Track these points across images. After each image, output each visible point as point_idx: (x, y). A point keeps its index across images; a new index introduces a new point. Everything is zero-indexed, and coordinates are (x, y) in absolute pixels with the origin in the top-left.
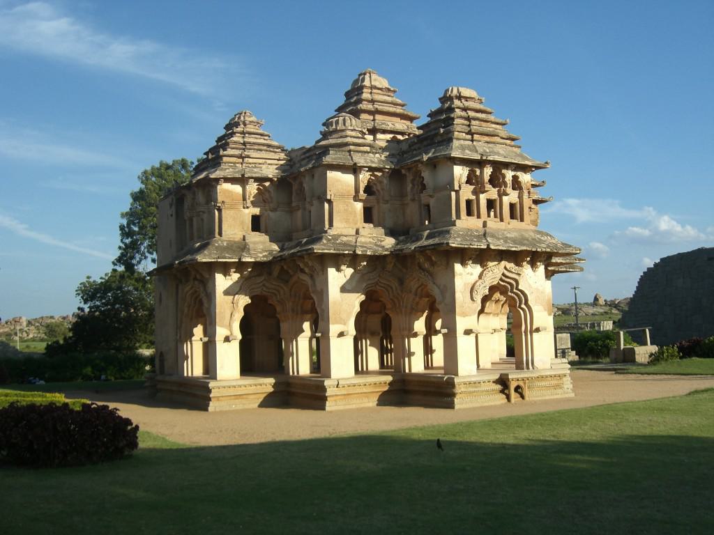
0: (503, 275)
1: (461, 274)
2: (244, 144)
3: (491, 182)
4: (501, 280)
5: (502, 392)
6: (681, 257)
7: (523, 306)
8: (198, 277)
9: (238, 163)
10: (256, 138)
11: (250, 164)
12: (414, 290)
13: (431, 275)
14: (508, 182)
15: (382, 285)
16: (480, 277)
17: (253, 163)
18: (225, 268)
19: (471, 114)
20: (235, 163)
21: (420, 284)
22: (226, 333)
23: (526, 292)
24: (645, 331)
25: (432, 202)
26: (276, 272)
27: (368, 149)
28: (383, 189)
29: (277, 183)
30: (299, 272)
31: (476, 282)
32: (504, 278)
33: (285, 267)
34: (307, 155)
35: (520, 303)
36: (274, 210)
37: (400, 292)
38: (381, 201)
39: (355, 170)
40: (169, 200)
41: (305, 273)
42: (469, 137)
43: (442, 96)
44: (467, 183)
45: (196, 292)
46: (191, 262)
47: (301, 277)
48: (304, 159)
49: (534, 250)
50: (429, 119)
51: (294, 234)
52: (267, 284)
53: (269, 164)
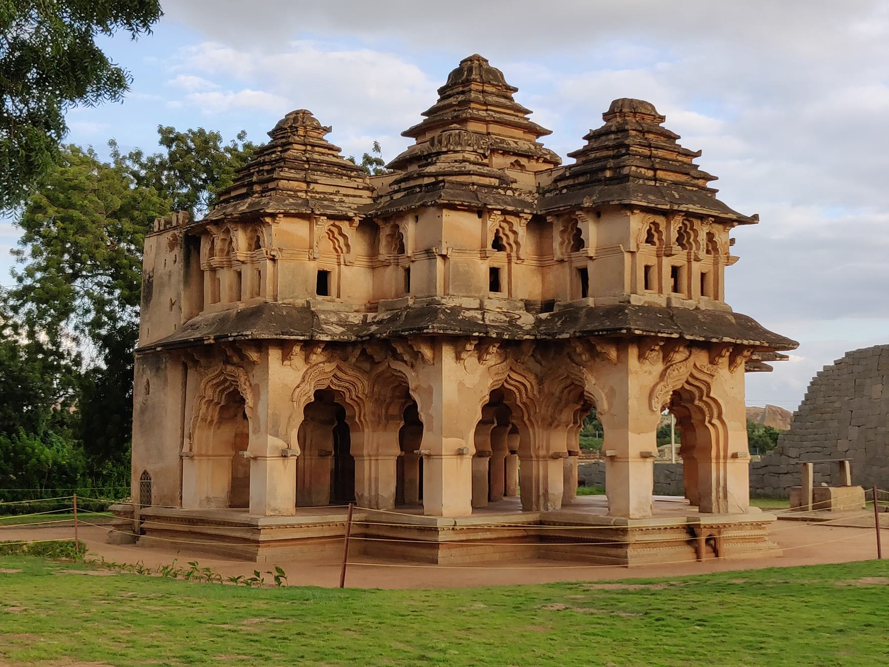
0: (692, 375)
1: (636, 373)
3: (679, 240)
4: (687, 382)
5: (689, 543)
7: (715, 421)
9: (301, 191)
10: (323, 154)
11: (318, 193)
12: (557, 394)
14: (701, 243)
15: (512, 382)
17: (322, 193)
21: (569, 382)
22: (281, 443)
23: (720, 401)
24: (842, 464)
25: (591, 268)
27: (496, 182)
30: (389, 358)
31: (657, 384)
32: (691, 380)
35: (711, 417)
38: (514, 259)
40: (168, 236)
42: (650, 173)
43: (607, 110)
44: (647, 242)
45: (225, 380)
49: (739, 342)
50: (586, 143)
52: (339, 374)
53: (344, 195)
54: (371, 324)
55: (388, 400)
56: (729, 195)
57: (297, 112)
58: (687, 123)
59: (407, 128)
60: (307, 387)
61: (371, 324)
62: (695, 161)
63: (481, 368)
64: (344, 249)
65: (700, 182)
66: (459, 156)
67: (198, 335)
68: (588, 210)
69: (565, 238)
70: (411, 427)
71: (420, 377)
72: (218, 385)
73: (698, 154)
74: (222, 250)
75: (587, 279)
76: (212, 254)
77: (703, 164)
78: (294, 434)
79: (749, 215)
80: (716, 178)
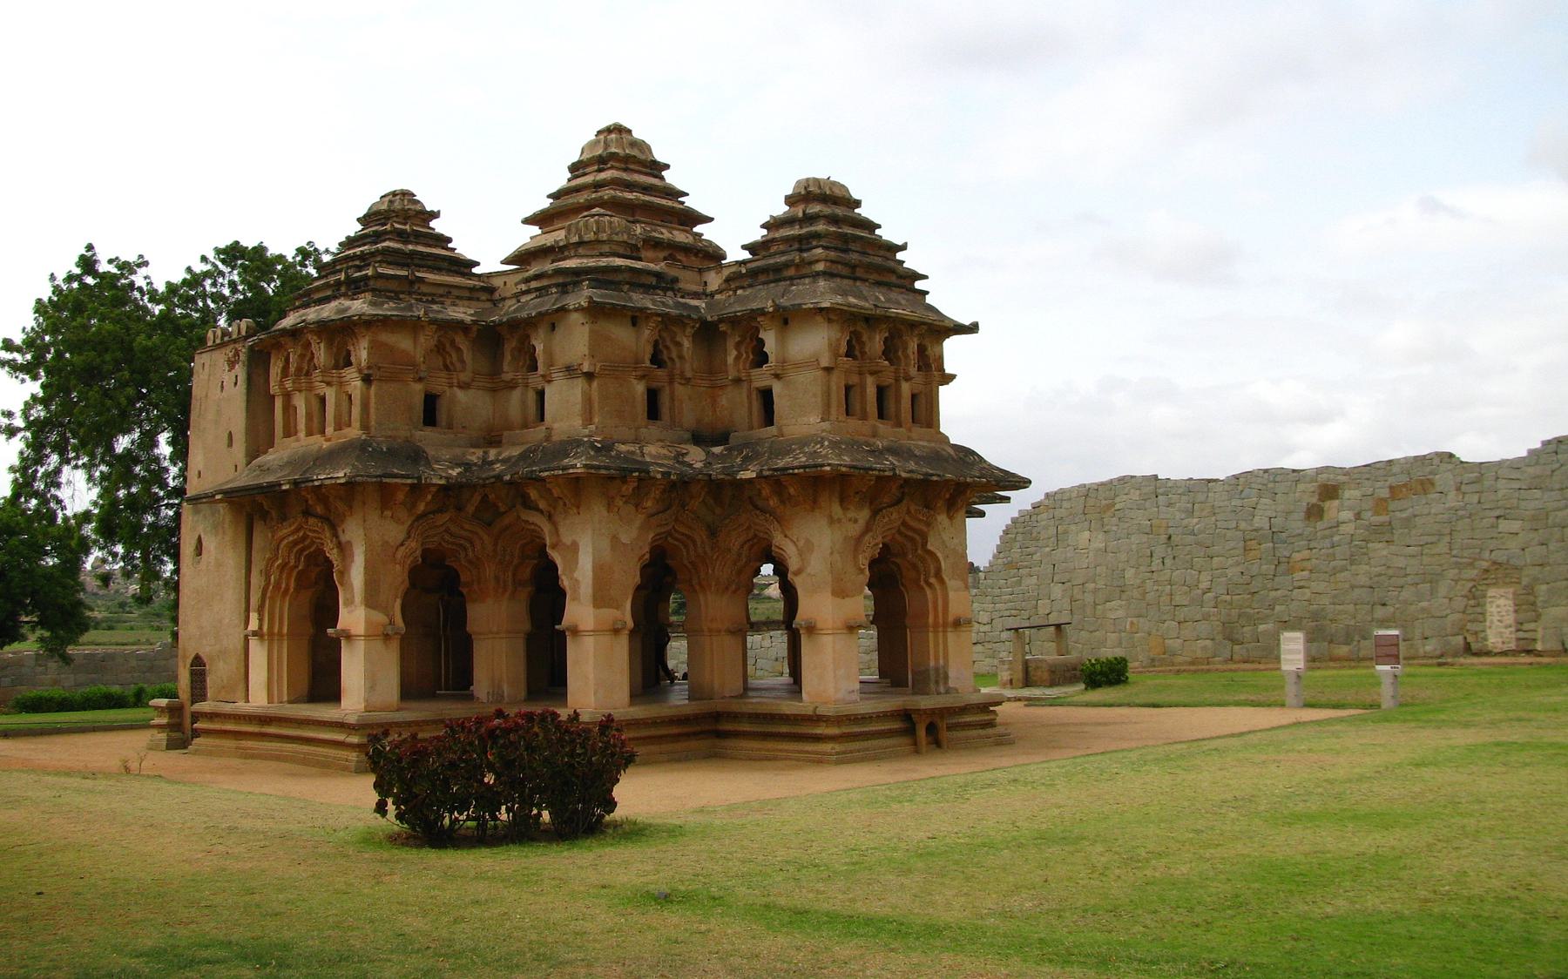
0: (904, 523)
1: (839, 521)
2: (413, 253)
6: (1087, 492)
8: (319, 509)
13: (779, 520)
16: (868, 529)
18: (385, 494)
19: (849, 230)
20: (397, 293)
25: (777, 389)
26: (471, 509)
27: (654, 281)
28: (681, 357)
29: (473, 334)
30: (519, 507)
33: (492, 497)
34: (534, 284)
36: (464, 386)
37: (708, 549)
39: (634, 322)
41: (537, 509)
46: (327, 482)
47: (524, 517)
48: (524, 293)
50: (765, 232)
51: (506, 433)
52: (453, 528)
54: (492, 463)
55: (516, 561)
56: (944, 297)
57: (394, 194)
58: (888, 211)
59: (529, 214)
60: (413, 544)
61: (492, 463)
62: (900, 256)
63: (639, 519)
64: (458, 366)
65: (906, 282)
66: (606, 248)
67: (271, 479)
68: (772, 316)
69: (743, 350)
70: (546, 596)
71: (562, 530)
72: (295, 543)
73: (904, 247)
74: (299, 369)
75: (772, 403)
76: (285, 372)
77: (909, 259)
78: (398, 603)
79: (967, 322)
80: (925, 277)
